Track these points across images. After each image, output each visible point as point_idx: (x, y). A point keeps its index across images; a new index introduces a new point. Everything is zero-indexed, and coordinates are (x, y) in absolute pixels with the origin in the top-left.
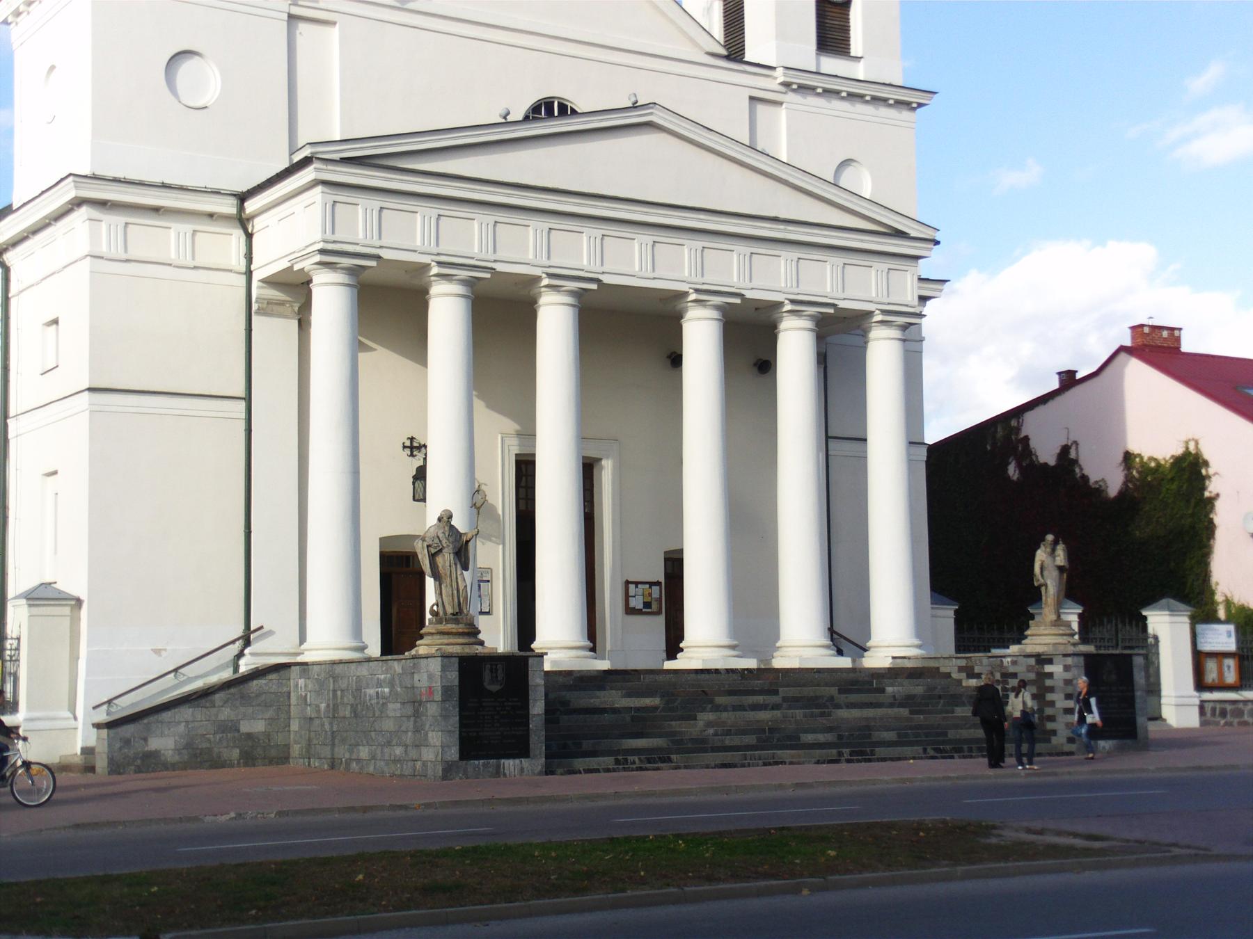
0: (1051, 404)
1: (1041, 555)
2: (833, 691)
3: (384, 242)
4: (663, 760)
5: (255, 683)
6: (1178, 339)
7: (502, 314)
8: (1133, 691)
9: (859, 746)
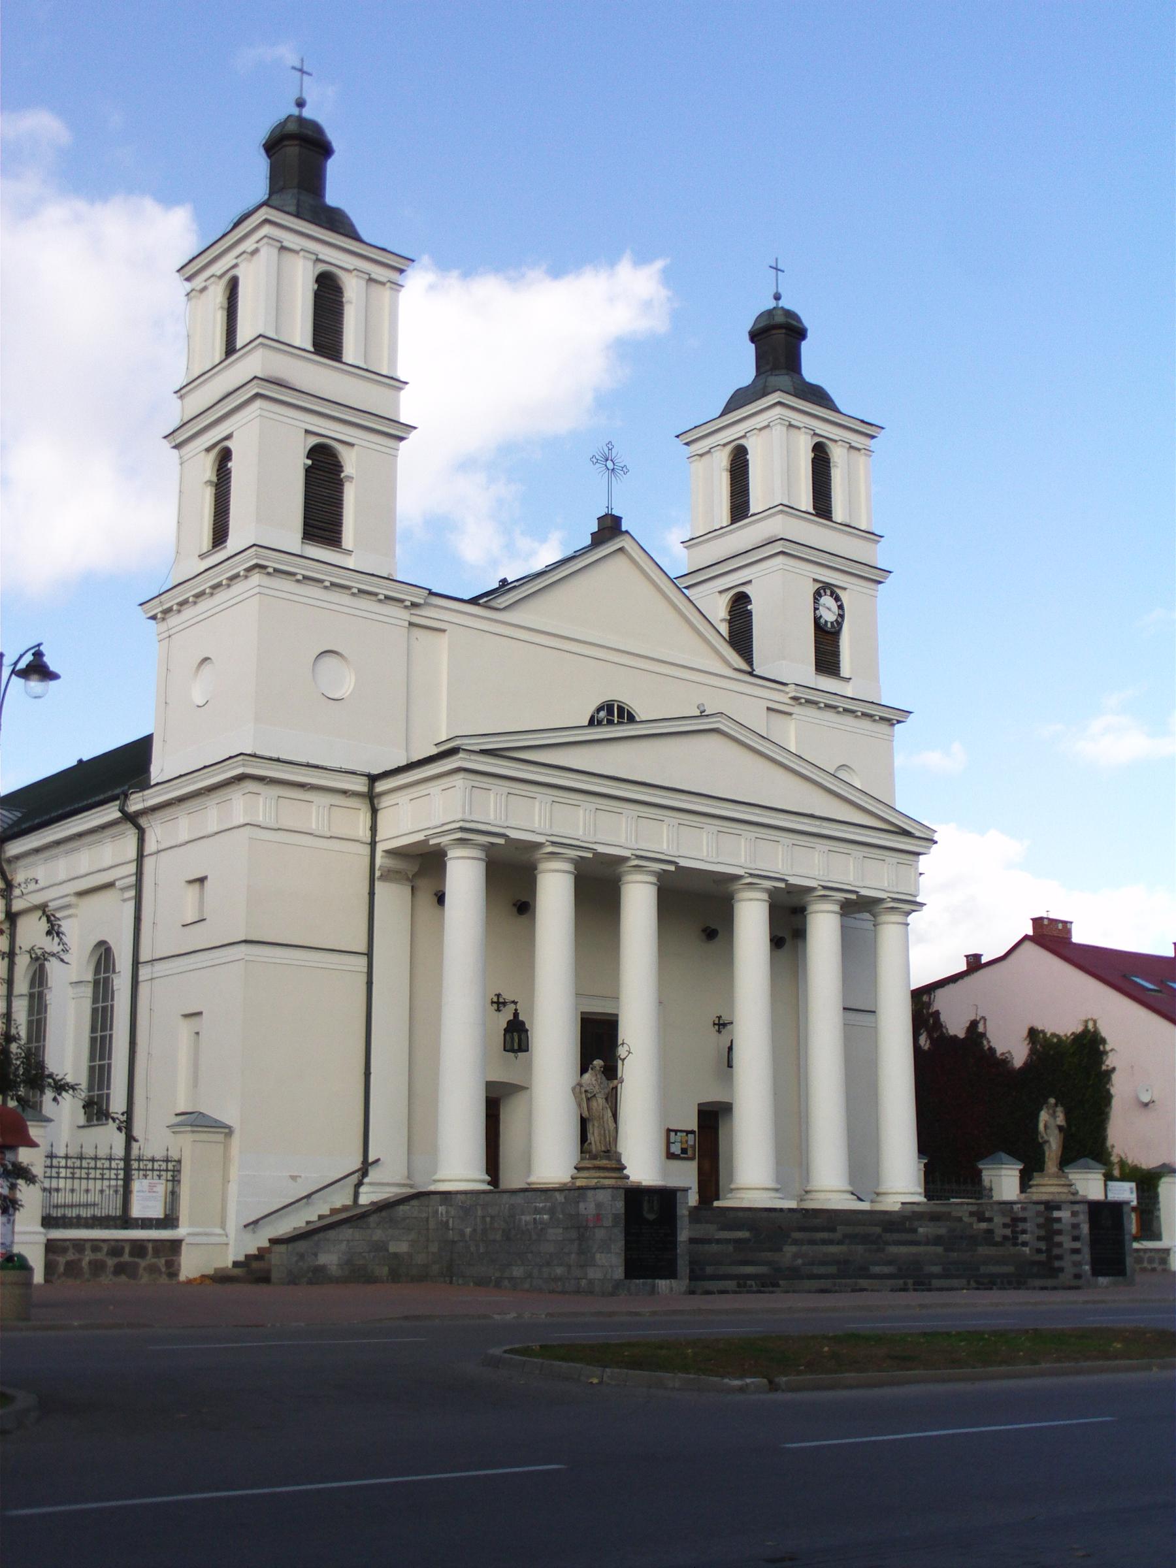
0: (960, 983)
1: (1044, 1116)
2: (878, 1230)
5: (402, 1209)
6: (1069, 932)
7: (598, 887)
9: (914, 1277)
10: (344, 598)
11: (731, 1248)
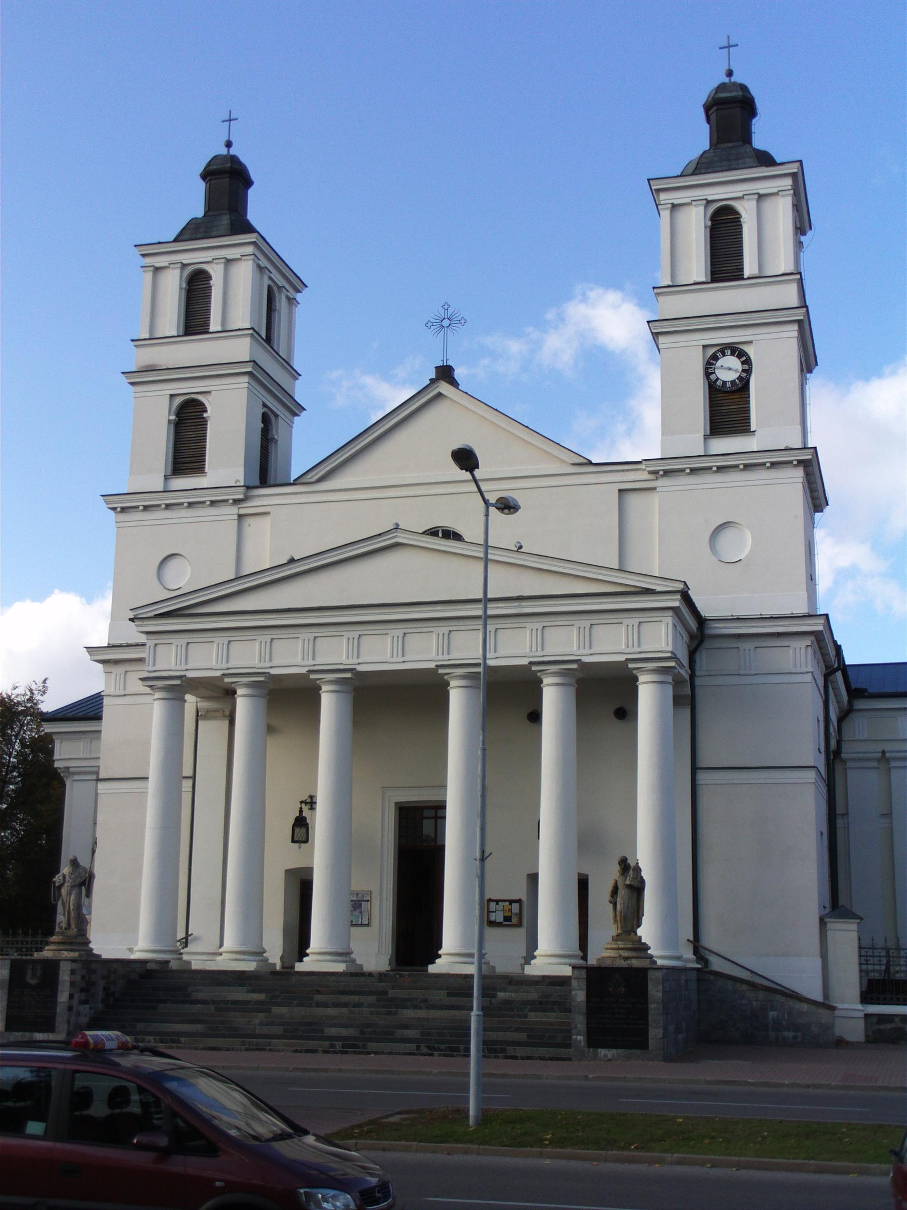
3: (189, 667)
4: (173, 1041)
8: (646, 1003)
10: (184, 513)
11: (212, 1008)
